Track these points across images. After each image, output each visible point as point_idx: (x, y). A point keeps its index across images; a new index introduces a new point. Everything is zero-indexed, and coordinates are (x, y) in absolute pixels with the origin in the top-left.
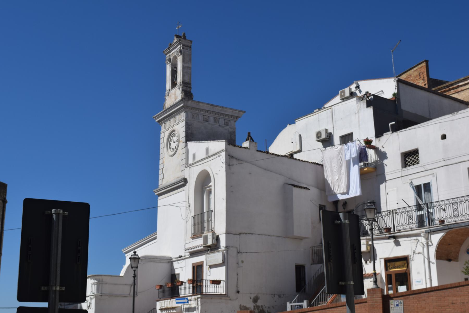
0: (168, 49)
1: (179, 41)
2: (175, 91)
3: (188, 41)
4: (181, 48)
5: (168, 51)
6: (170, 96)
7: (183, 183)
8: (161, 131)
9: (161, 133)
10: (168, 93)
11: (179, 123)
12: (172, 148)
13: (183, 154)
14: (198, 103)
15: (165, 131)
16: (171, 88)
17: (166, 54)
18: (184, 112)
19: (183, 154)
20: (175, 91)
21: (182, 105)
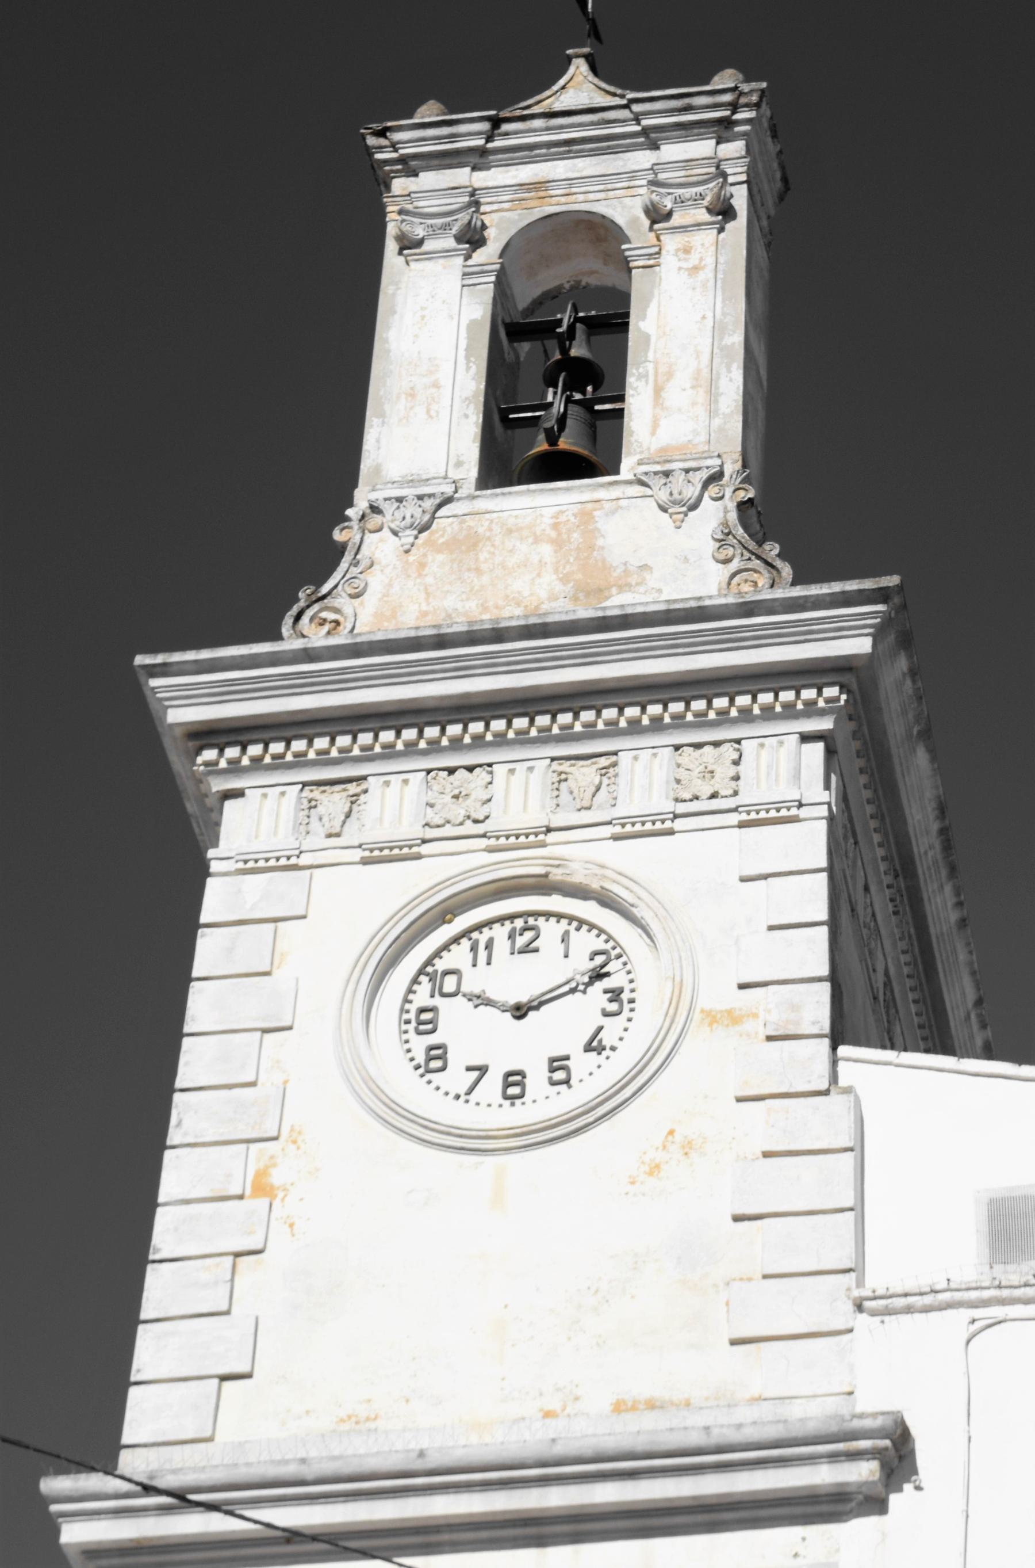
0: (485, 126)
1: (727, 98)
2: (586, 518)
3: (775, 165)
4: (737, 172)
5: (482, 142)
6: (471, 543)
7: (866, 1471)
8: (215, 844)
9: (215, 866)
10: (429, 504)
11: (679, 824)
12: (457, 1060)
13: (767, 1155)
14: (915, 731)
15: (305, 860)
16: (471, 471)
17: (410, 166)
18: (806, 738)
19: (767, 1155)
20: (586, 518)
21: (861, 645)
